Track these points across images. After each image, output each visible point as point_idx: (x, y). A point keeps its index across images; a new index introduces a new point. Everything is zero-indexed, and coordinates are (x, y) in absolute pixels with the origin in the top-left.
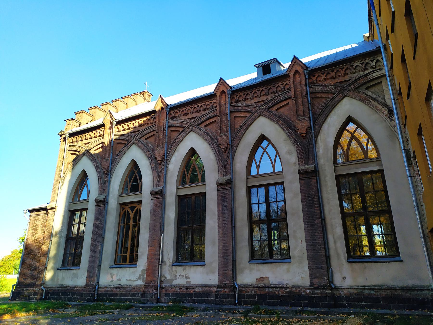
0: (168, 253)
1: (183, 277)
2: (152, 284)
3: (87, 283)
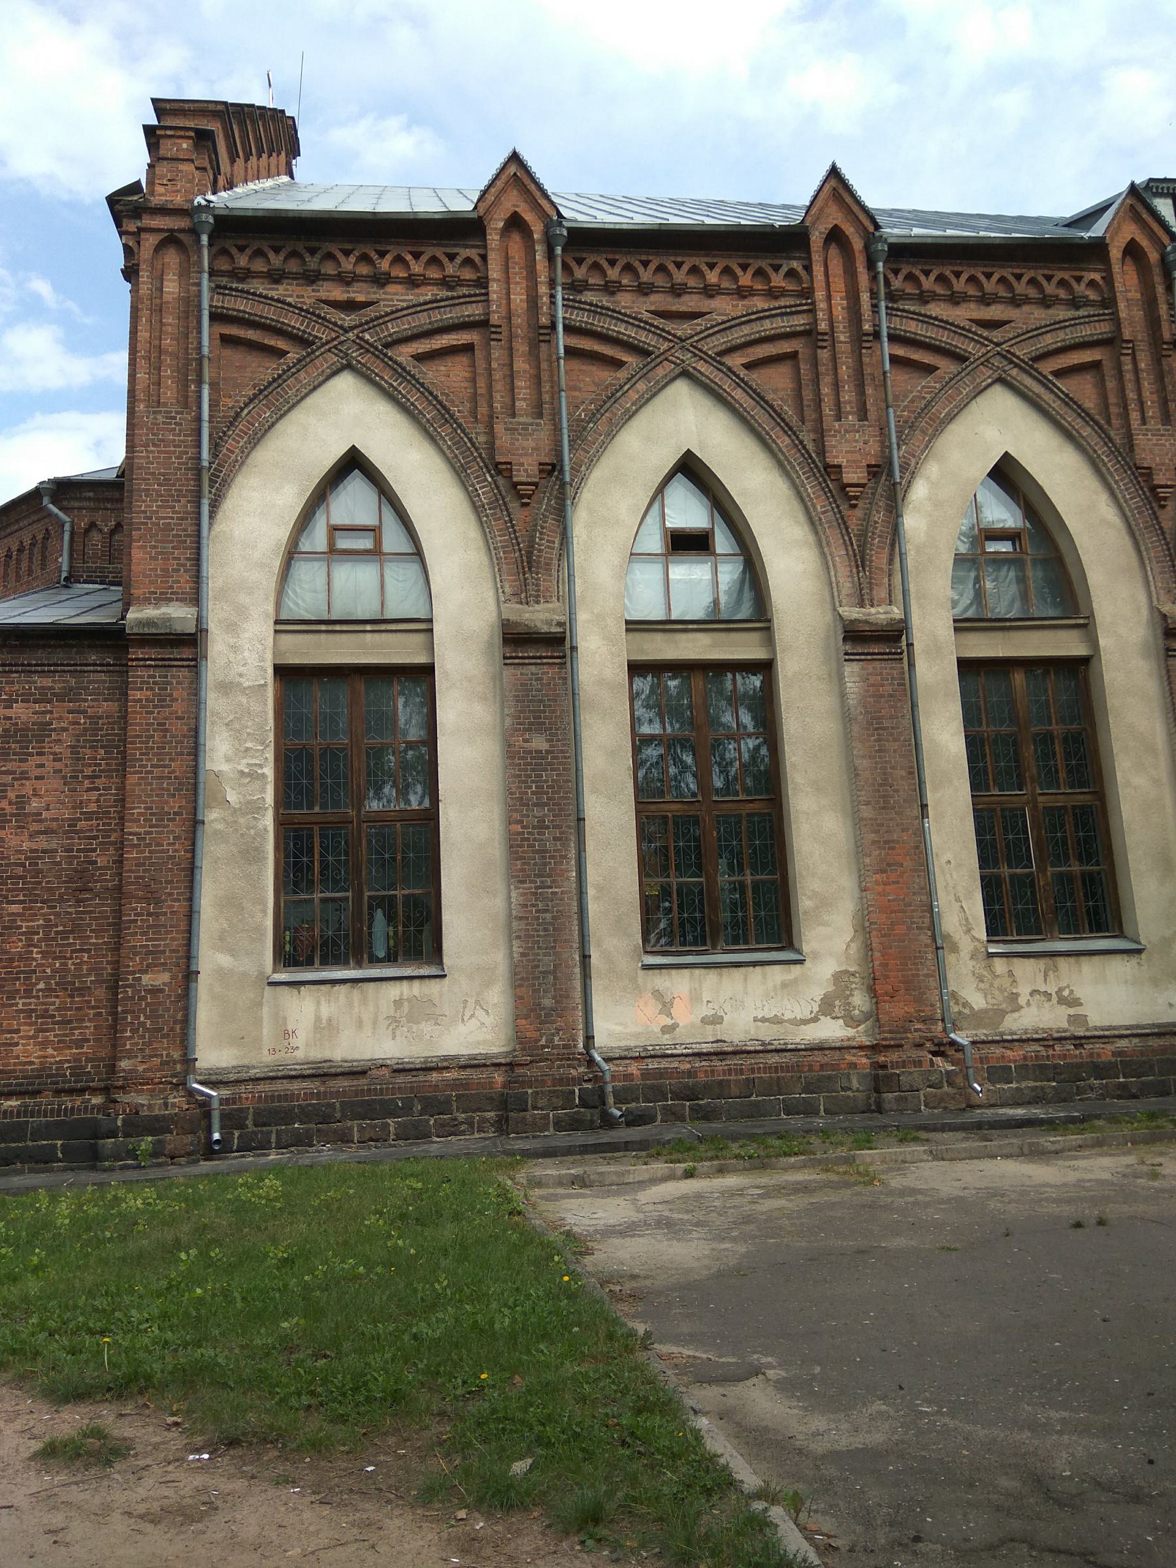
0: (958, 900)
1: (1049, 1000)
2: (916, 1030)
3: (520, 1039)
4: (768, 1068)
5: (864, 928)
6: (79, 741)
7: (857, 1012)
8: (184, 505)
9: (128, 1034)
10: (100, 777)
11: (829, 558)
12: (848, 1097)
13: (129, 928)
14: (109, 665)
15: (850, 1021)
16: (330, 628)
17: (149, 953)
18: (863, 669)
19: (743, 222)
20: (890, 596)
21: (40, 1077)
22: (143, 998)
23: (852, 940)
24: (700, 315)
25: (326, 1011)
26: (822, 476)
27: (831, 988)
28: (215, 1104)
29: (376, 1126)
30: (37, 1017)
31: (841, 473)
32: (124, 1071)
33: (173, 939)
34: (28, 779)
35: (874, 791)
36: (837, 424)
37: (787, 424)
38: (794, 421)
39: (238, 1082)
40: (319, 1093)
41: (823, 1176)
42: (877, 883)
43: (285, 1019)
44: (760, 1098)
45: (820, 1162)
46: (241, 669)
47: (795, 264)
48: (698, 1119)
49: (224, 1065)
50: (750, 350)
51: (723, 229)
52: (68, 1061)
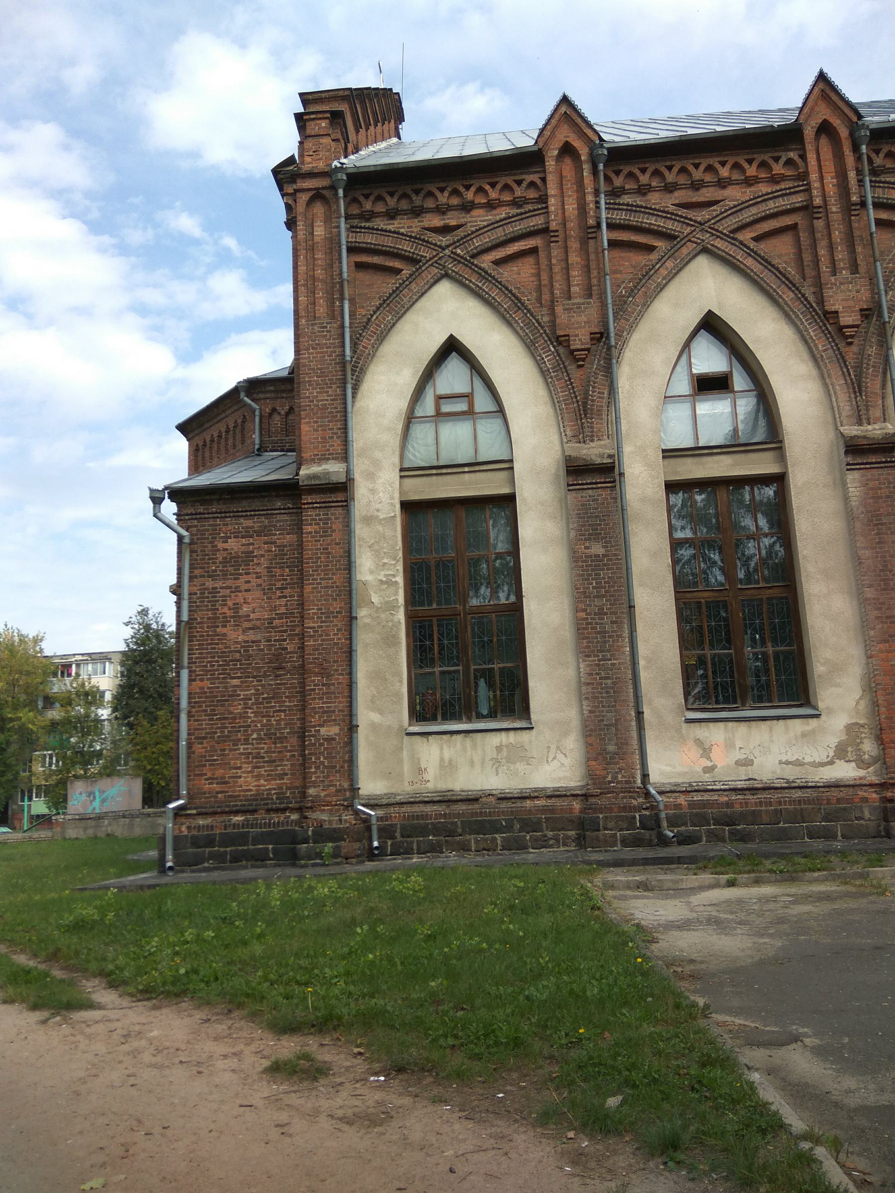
3: (591, 775)
4: (792, 801)
5: (870, 688)
6: (272, 563)
7: (866, 756)
8: (334, 390)
9: (313, 770)
10: (286, 588)
11: (831, 387)
12: (862, 825)
13: (310, 695)
14: (289, 508)
15: (861, 763)
16: (439, 471)
17: (326, 712)
18: (863, 476)
19: (748, 126)
20: (884, 415)
21: (257, 800)
22: (322, 745)
23: (861, 698)
24: (716, 202)
25: (447, 754)
26: (822, 321)
27: (844, 737)
28: (374, 821)
29: (486, 840)
30: (253, 758)
31: (838, 317)
32: (312, 796)
33: (340, 702)
34: (240, 591)
35: (875, 576)
36: (833, 279)
37: (791, 282)
38: (797, 279)
39: (388, 805)
40: (445, 814)
41: (842, 888)
42: (881, 651)
43: (419, 759)
44: (787, 825)
45: (839, 876)
46: (378, 506)
47: (792, 155)
48: (737, 840)
49: (379, 793)
50: (758, 226)
51: (731, 133)
52: (275, 789)
